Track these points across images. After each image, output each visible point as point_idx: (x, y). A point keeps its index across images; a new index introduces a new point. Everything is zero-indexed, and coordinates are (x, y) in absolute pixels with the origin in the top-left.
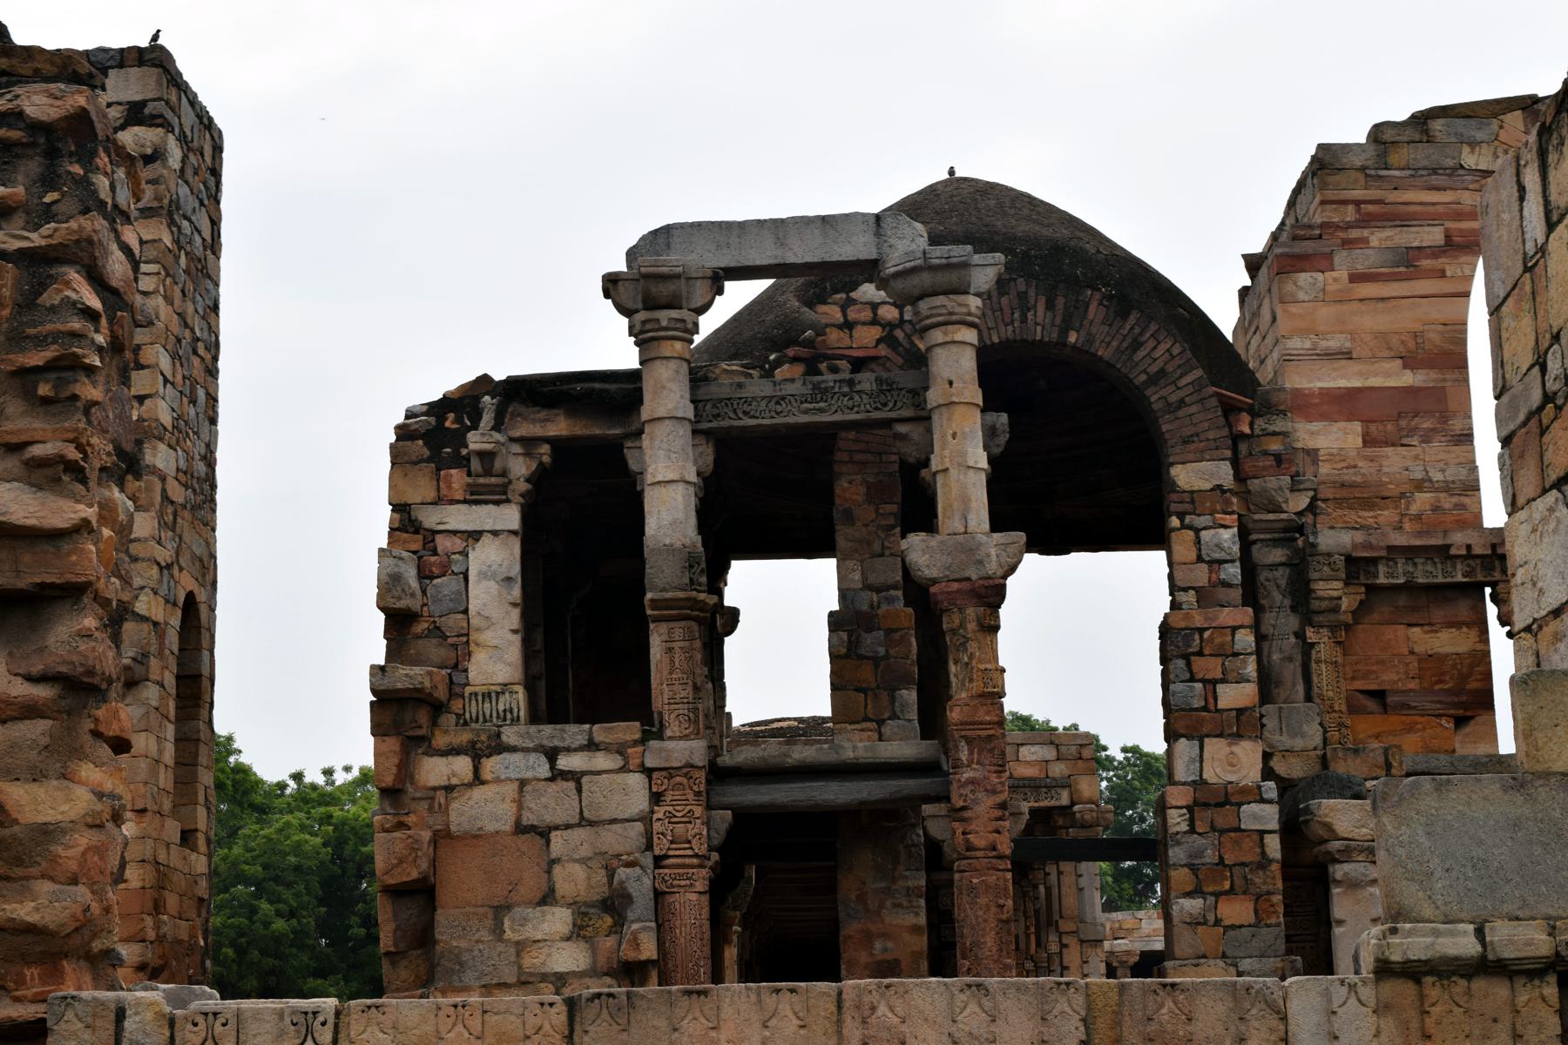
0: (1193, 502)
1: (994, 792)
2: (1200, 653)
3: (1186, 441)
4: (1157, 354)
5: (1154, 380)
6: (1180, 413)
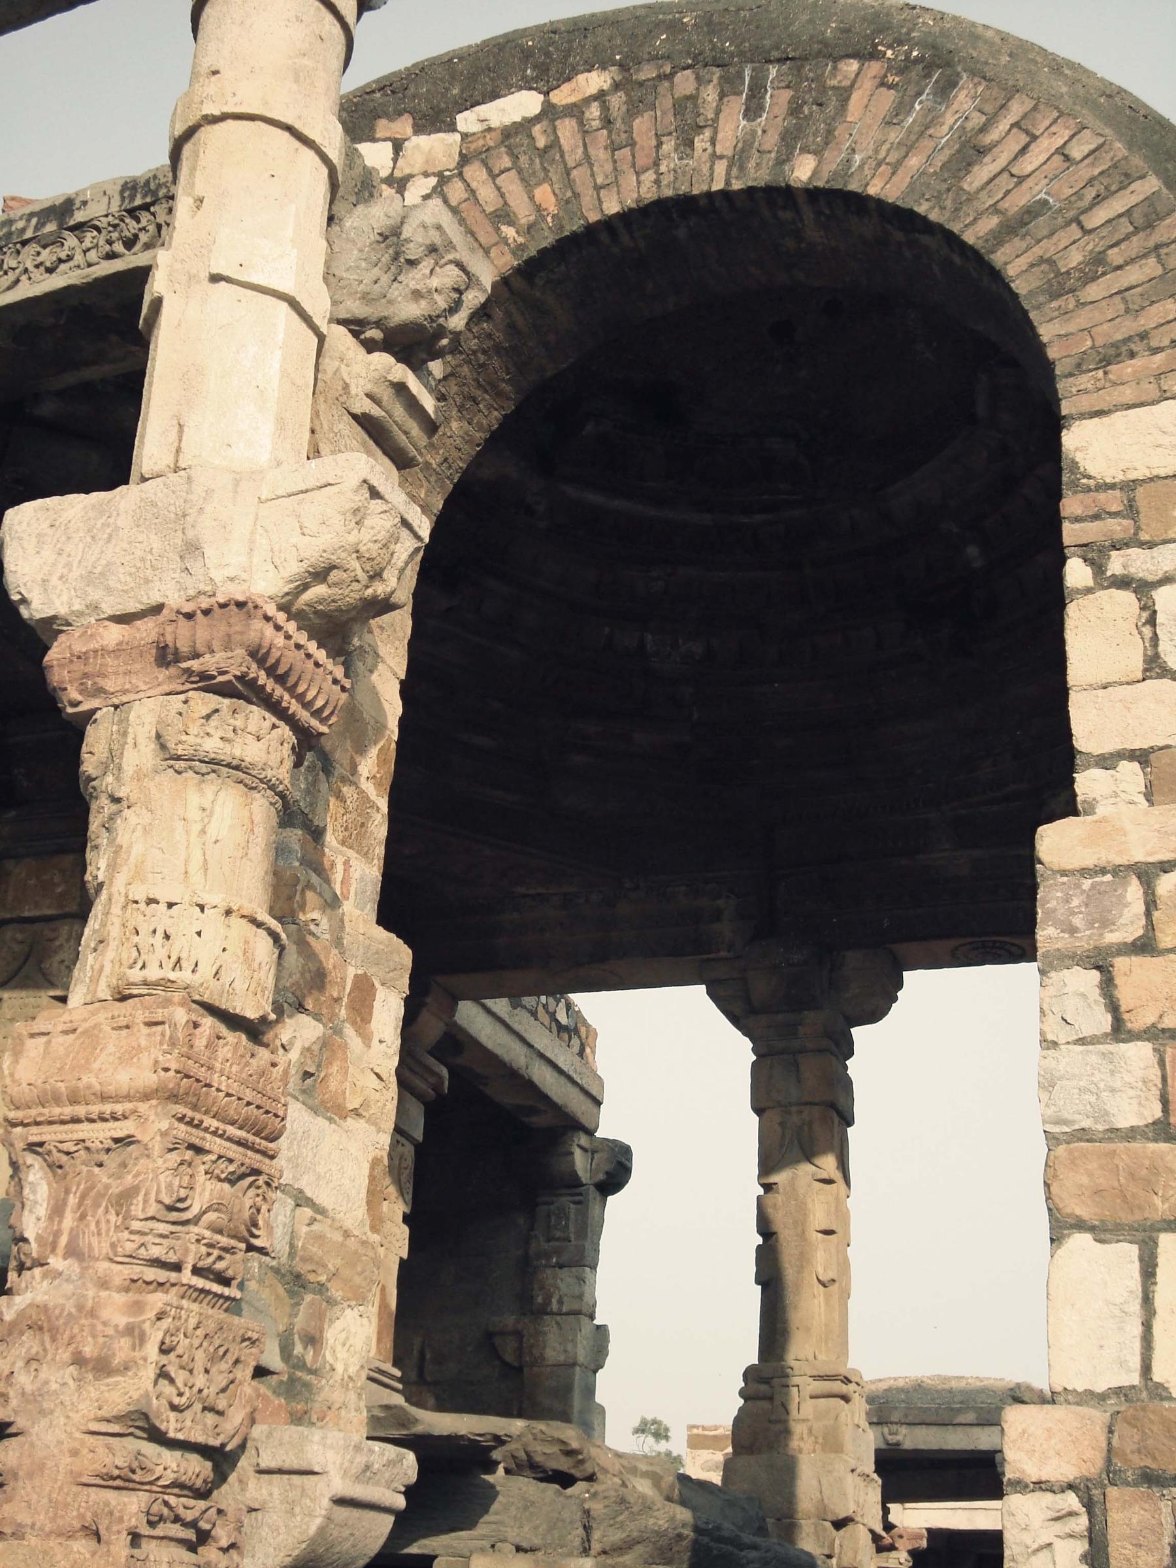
0: (1131, 511)
1: (102, 1367)
2: (1145, 946)
3: (1109, 357)
4: (1028, 164)
5: (1015, 226)
6: (1093, 291)
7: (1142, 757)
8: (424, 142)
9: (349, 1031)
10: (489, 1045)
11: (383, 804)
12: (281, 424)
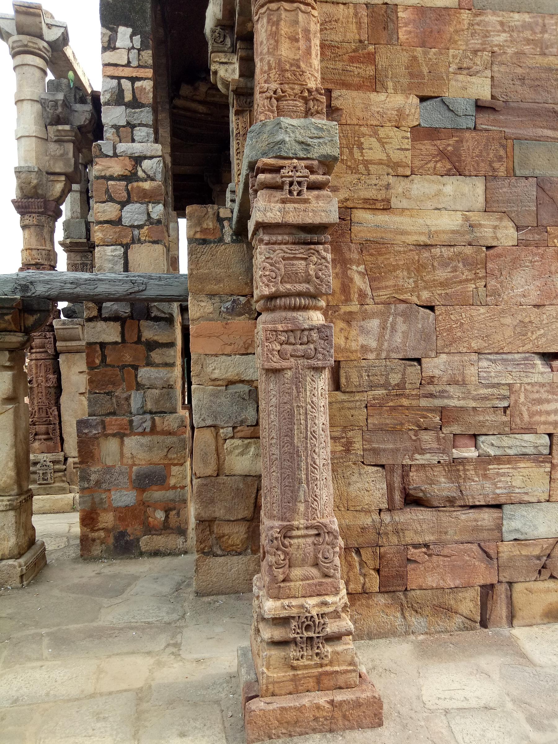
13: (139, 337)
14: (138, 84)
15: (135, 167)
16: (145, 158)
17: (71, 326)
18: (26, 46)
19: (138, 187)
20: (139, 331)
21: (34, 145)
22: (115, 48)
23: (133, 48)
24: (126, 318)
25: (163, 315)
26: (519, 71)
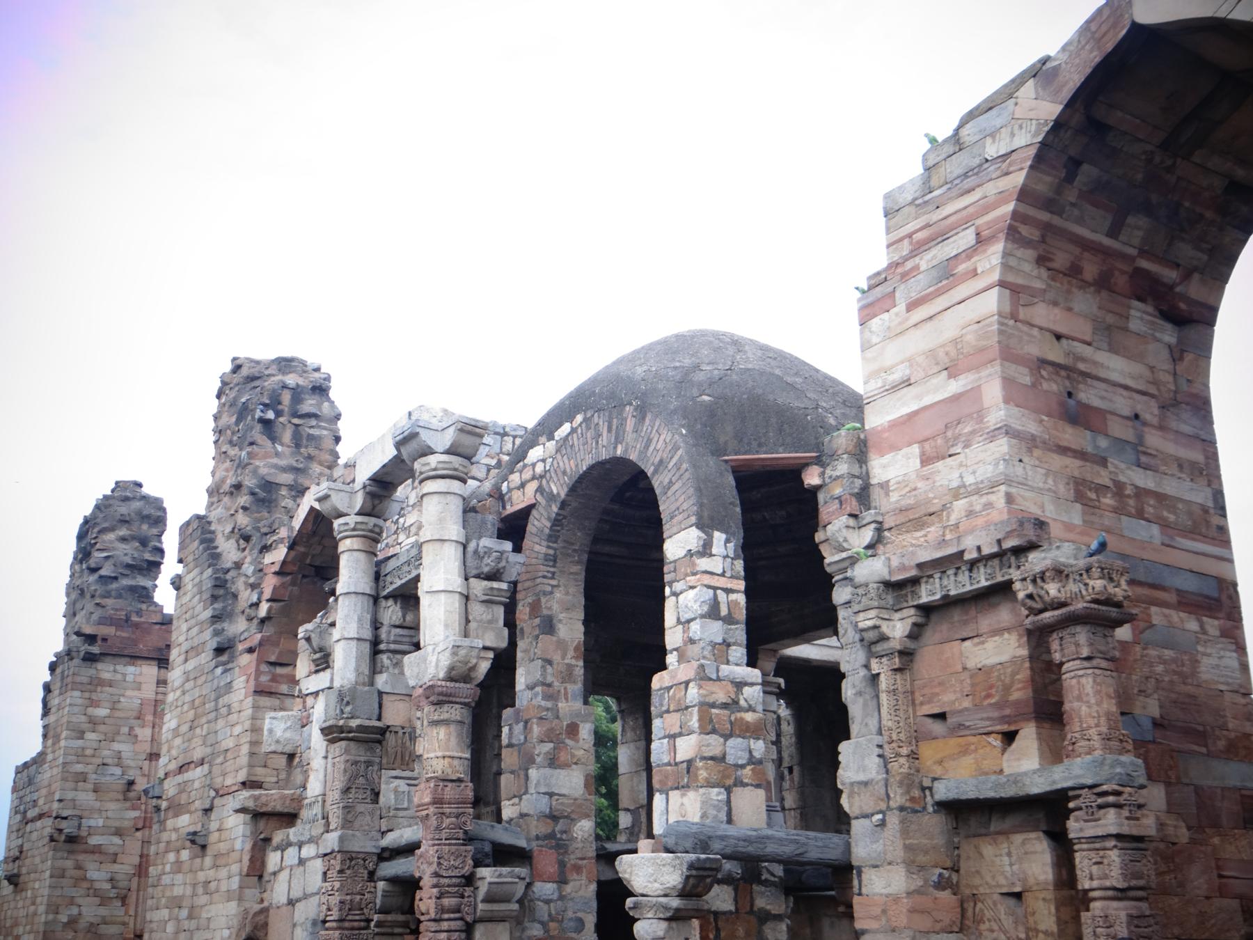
7: (676, 649)
8: (548, 444)
9: (568, 741)
10: (818, 657)
11: (581, 663)
12: (446, 626)
13: (752, 905)
14: (733, 597)
15: (737, 694)
16: (746, 684)
17: (510, 880)
18: (455, 470)
19: (742, 719)
20: (752, 897)
21: (457, 605)
22: (711, 555)
23: (727, 556)
24: (738, 880)
25: (772, 879)
26: (1173, 696)
